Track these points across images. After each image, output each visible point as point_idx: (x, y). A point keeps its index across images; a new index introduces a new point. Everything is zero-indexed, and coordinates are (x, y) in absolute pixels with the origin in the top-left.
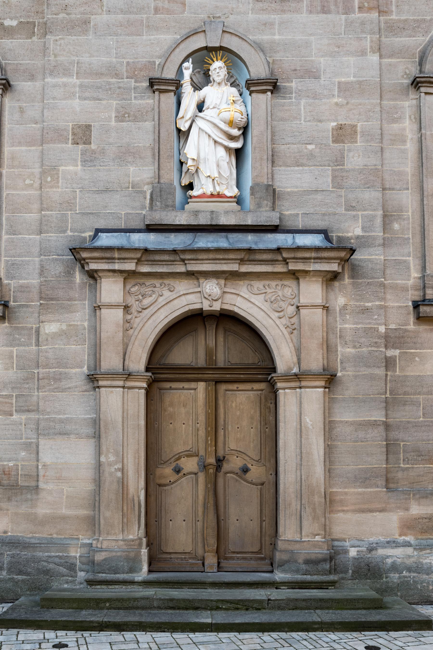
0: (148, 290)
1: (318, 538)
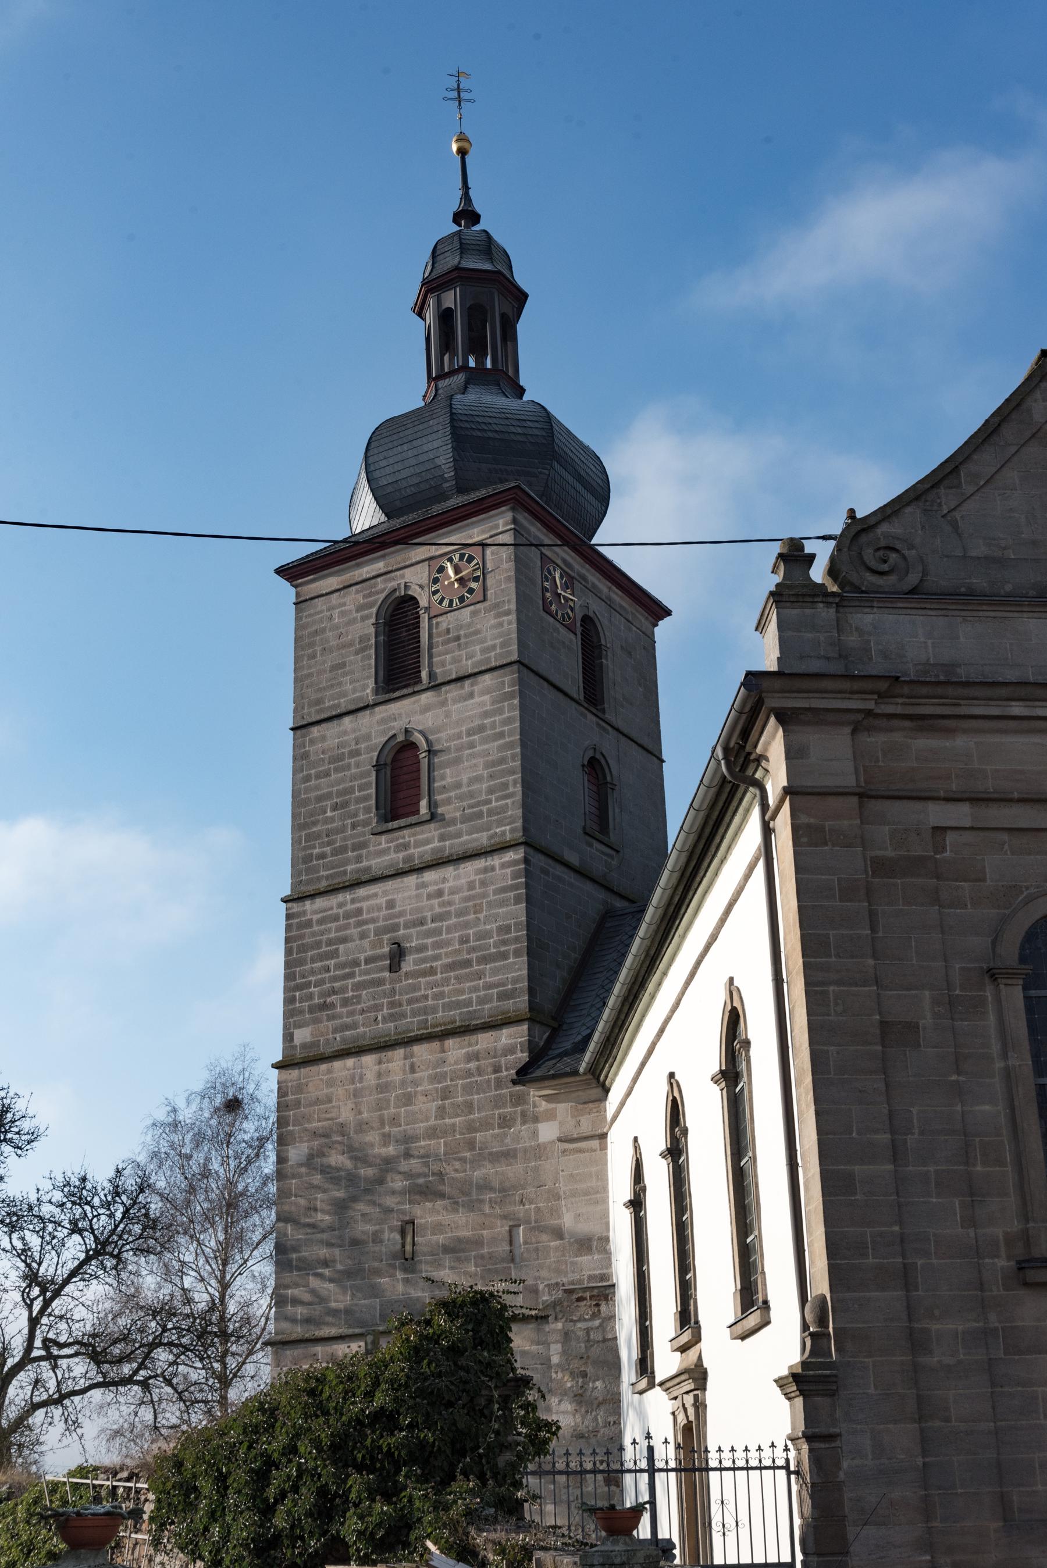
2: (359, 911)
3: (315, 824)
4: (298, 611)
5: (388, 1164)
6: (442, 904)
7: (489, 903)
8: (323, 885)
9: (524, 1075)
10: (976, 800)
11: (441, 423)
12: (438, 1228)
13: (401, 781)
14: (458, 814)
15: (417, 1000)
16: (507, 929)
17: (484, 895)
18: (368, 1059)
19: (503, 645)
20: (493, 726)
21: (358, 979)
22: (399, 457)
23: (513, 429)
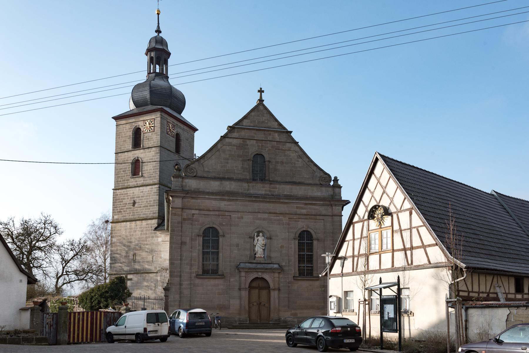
2: (127, 194)
11: (147, 88)
13: (136, 167)
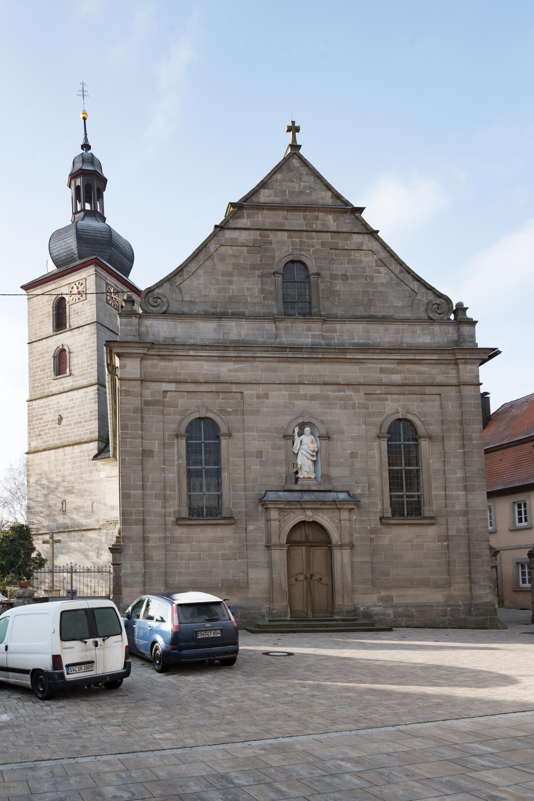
0: (286, 514)
1: (350, 604)
2: (49, 405)
3: (35, 376)
4: (29, 302)
5: (58, 484)
6: (73, 403)
7: (87, 403)
8: (38, 396)
9: (96, 457)
10: (177, 382)
11: (73, 232)
12: (72, 503)
13: (61, 362)
14: (78, 374)
15: (66, 434)
16: (92, 412)
17: (86, 401)
18: (52, 452)
19: (92, 316)
20: (89, 344)
21: (49, 427)
22: (60, 245)
23: (98, 235)
